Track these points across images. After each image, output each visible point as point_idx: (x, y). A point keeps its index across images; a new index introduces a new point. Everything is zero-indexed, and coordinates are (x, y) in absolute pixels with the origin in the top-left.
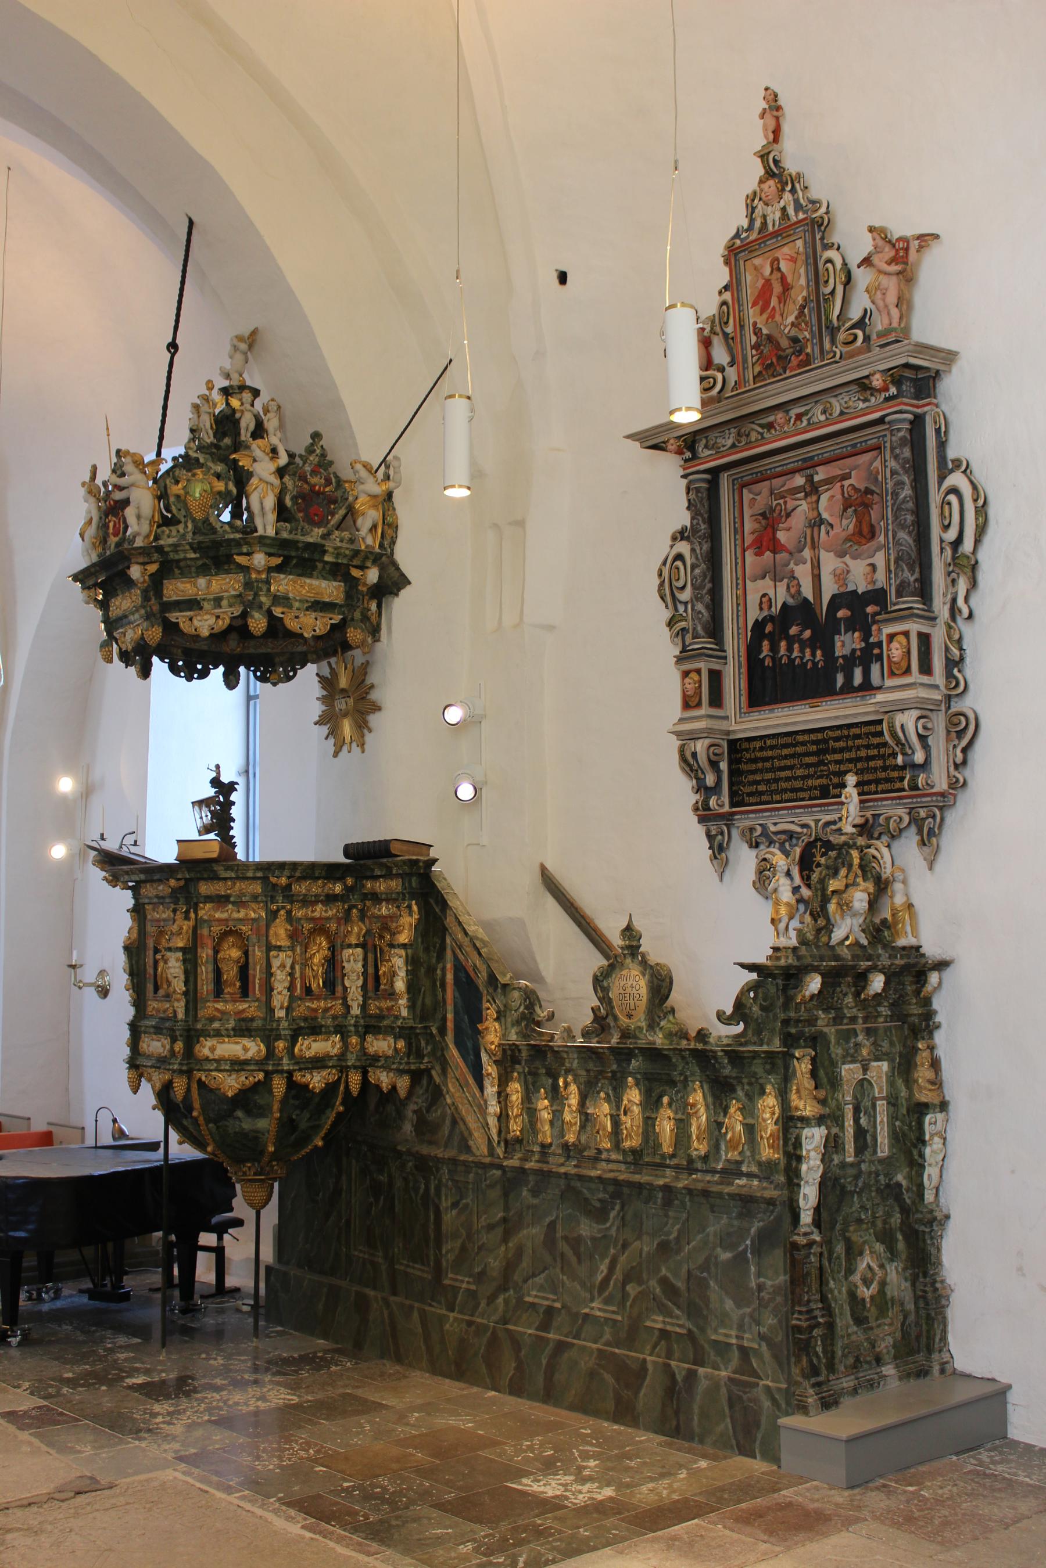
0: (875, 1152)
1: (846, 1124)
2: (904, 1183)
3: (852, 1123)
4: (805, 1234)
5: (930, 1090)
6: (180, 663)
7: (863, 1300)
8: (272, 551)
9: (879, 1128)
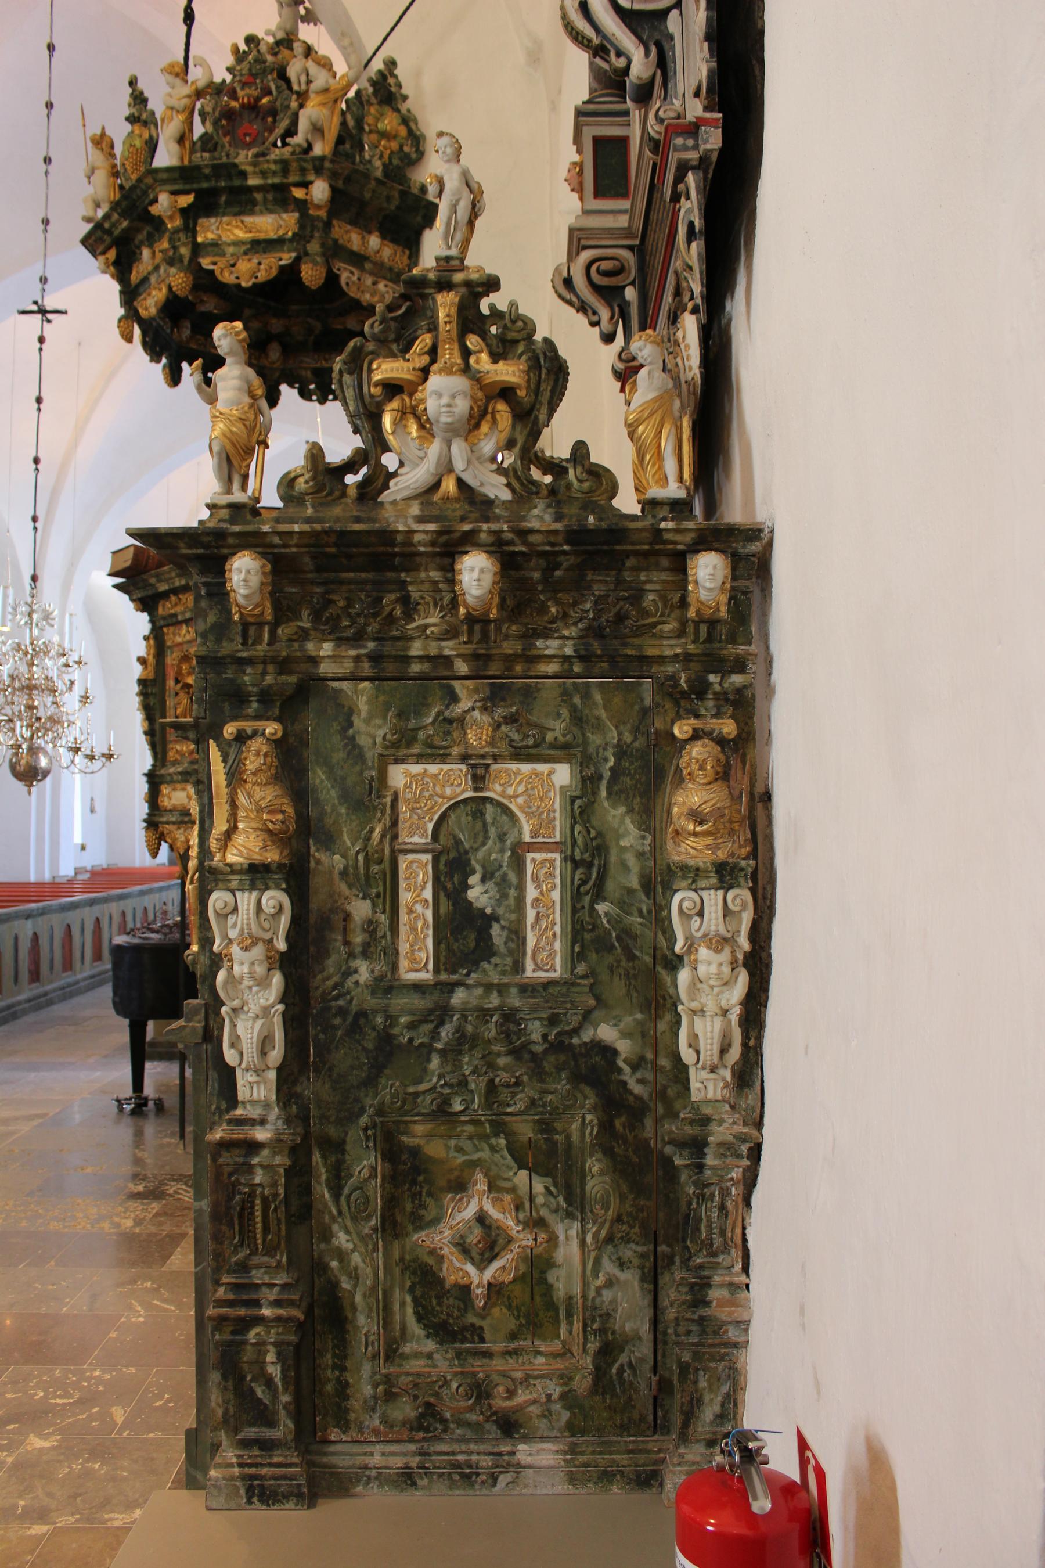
0: (518, 967)
1: (405, 897)
2: (624, 1047)
3: (428, 894)
4: (240, 1122)
5: (695, 834)
6: (312, 387)
7: (465, 1291)
8: (176, 187)
9: (531, 915)
